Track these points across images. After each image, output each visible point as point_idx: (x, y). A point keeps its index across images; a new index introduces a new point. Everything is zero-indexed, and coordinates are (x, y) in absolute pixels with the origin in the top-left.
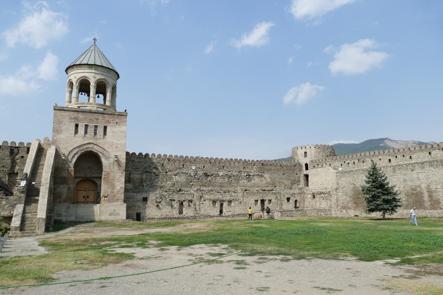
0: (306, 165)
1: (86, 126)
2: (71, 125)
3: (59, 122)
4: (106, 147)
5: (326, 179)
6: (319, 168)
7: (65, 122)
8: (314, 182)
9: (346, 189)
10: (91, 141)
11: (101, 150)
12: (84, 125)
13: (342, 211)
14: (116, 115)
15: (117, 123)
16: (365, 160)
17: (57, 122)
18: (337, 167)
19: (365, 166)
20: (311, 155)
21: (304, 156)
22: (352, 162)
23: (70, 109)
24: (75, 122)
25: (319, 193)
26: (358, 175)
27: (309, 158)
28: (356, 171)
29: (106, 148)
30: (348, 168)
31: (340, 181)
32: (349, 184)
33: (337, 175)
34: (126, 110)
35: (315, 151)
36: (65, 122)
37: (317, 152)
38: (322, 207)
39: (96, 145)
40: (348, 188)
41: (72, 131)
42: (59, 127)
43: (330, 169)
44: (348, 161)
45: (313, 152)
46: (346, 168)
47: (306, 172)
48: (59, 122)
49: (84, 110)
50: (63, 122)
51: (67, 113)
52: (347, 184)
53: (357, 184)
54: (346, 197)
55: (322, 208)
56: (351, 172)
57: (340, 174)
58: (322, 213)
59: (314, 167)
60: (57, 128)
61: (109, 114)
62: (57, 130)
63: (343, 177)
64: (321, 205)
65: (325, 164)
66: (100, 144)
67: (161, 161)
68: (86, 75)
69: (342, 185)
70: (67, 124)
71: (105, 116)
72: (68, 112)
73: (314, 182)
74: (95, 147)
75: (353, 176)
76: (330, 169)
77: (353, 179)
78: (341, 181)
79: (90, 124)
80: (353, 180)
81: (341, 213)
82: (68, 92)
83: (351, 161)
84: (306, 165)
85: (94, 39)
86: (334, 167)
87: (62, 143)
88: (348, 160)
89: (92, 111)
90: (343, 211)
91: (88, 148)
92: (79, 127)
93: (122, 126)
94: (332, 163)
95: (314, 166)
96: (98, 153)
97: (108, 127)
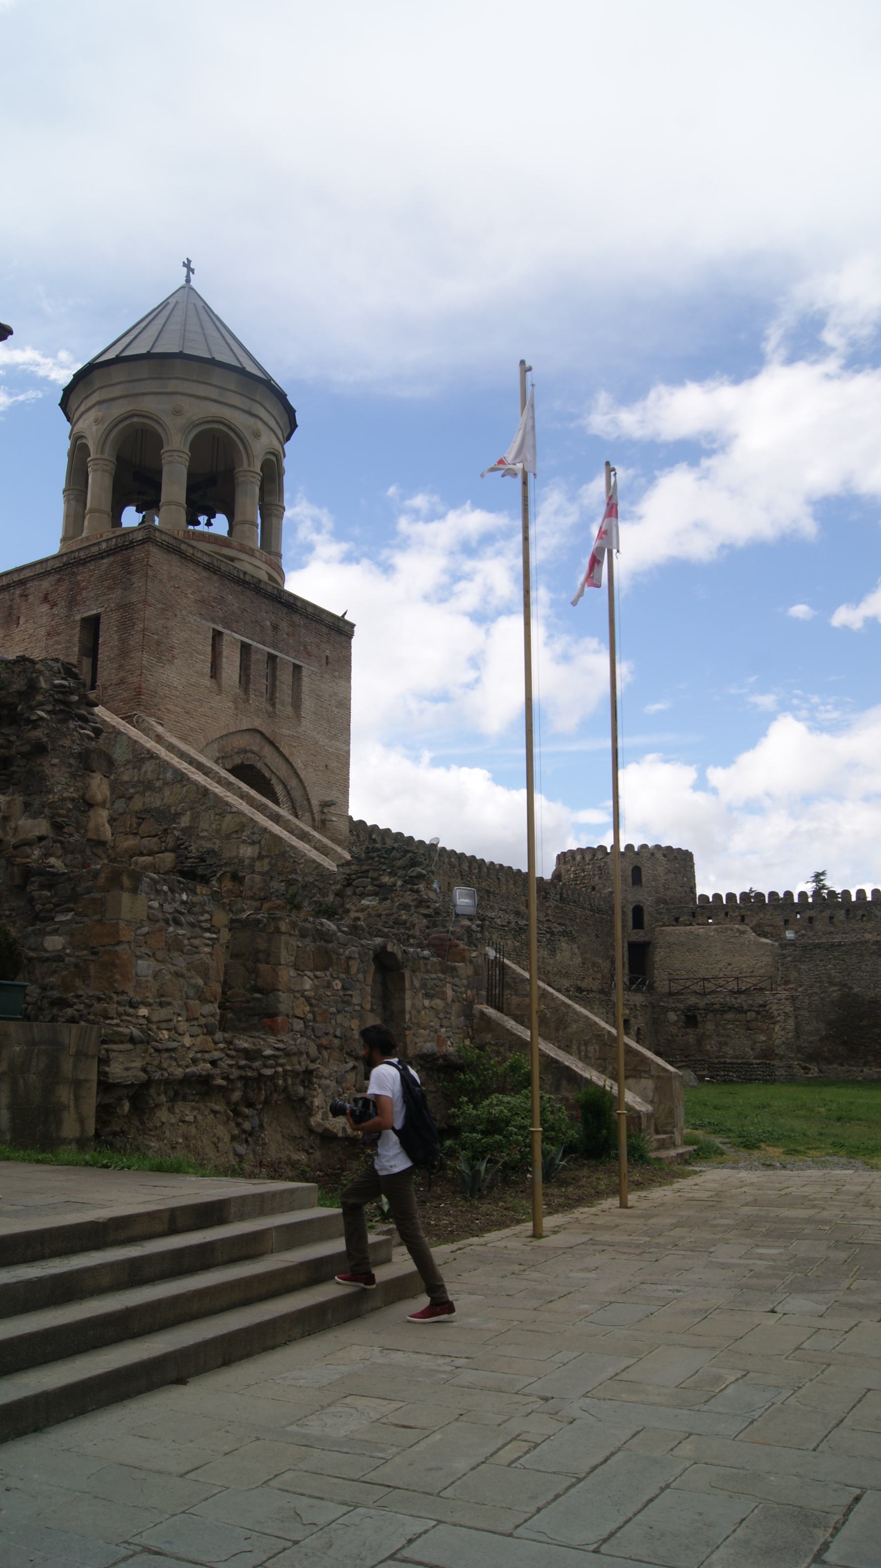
0: (638, 912)
1: (245, 649)
2: (199, 633)
3: (164, 606)
4: (299, 760)
5: (729, 964)
6: (698, 924)
7: (184, 613)
8: (678, 972)
9: (816, 998)
10: (257, 723)
11: (283, 771)
12: (239, 644)
13: (809, 1069)
14: (326, 625)
15: (327, 663)
16: (871, 912)
17: (159, 606)
18: (771, 928)
19: (870, 933)
20: (654, 880)
21: (630, 880)
22: (824, 914)
23: (199, 555)
24: (214, 622)
25: (715, 1006)
26: (860, 958)
27: (647, 890)
28: (854, 944)
29: (298, 763)
30: (810, 934)
31: (796, 974)
32: (827, 985)
33: (784, 954)
34: (345, 613)
35: (666, 866)
36: (184, 613)
37: (669, 871)
38: (729, 1056)
39: (272, 743)
40: (822, 995)
41: (203, 661)
42: (165, 631)
43: (744, 932)
44: (812, 912)
45: (661, 870)
46: (803, 932)
47: (639, 936)
48: (164, 606)
49: (242, 576)
50: (178, 612)
51: (189, 574)
52: (818, 985)
53: (854, 986)
54: (817, 1023)
55: (731, 1058)
56: (837, 946)
57: (796, 951)
58: (731, 1074)
59: (677, 920)
60: (157, 634)
61: (307, 617)
62: (158, 643)
63: (807, 959)
64: (725, 1049)
65: (722, 915)
66: (283, 743)
67: (356, 846)
68: (227, 414)
69: (801, 986)
70: (190, 622)
71: (297, 618)
72: (191, 566)
73: (678, 972)
74: (267, 750)
75: (842, 960)
76: (744, 932)
77: (840, 969)
78: (799, 974)
79: (254, 644)
80: (840, 973)
81: (807, 1073)
82: (106, 468)
83: (822, 911)
84: (638, 912)
85: (186, 262)
86: (759, 925)
87: (171, 707)
88: (810, 909)
89: (262, 586)
90: (811, 1067)
91: (245, 751)
92: (226, 651)
93: (340, 677)
94: (749, 913)
95: (678, 916)
96: (274, 781)
97: (304, 673)
